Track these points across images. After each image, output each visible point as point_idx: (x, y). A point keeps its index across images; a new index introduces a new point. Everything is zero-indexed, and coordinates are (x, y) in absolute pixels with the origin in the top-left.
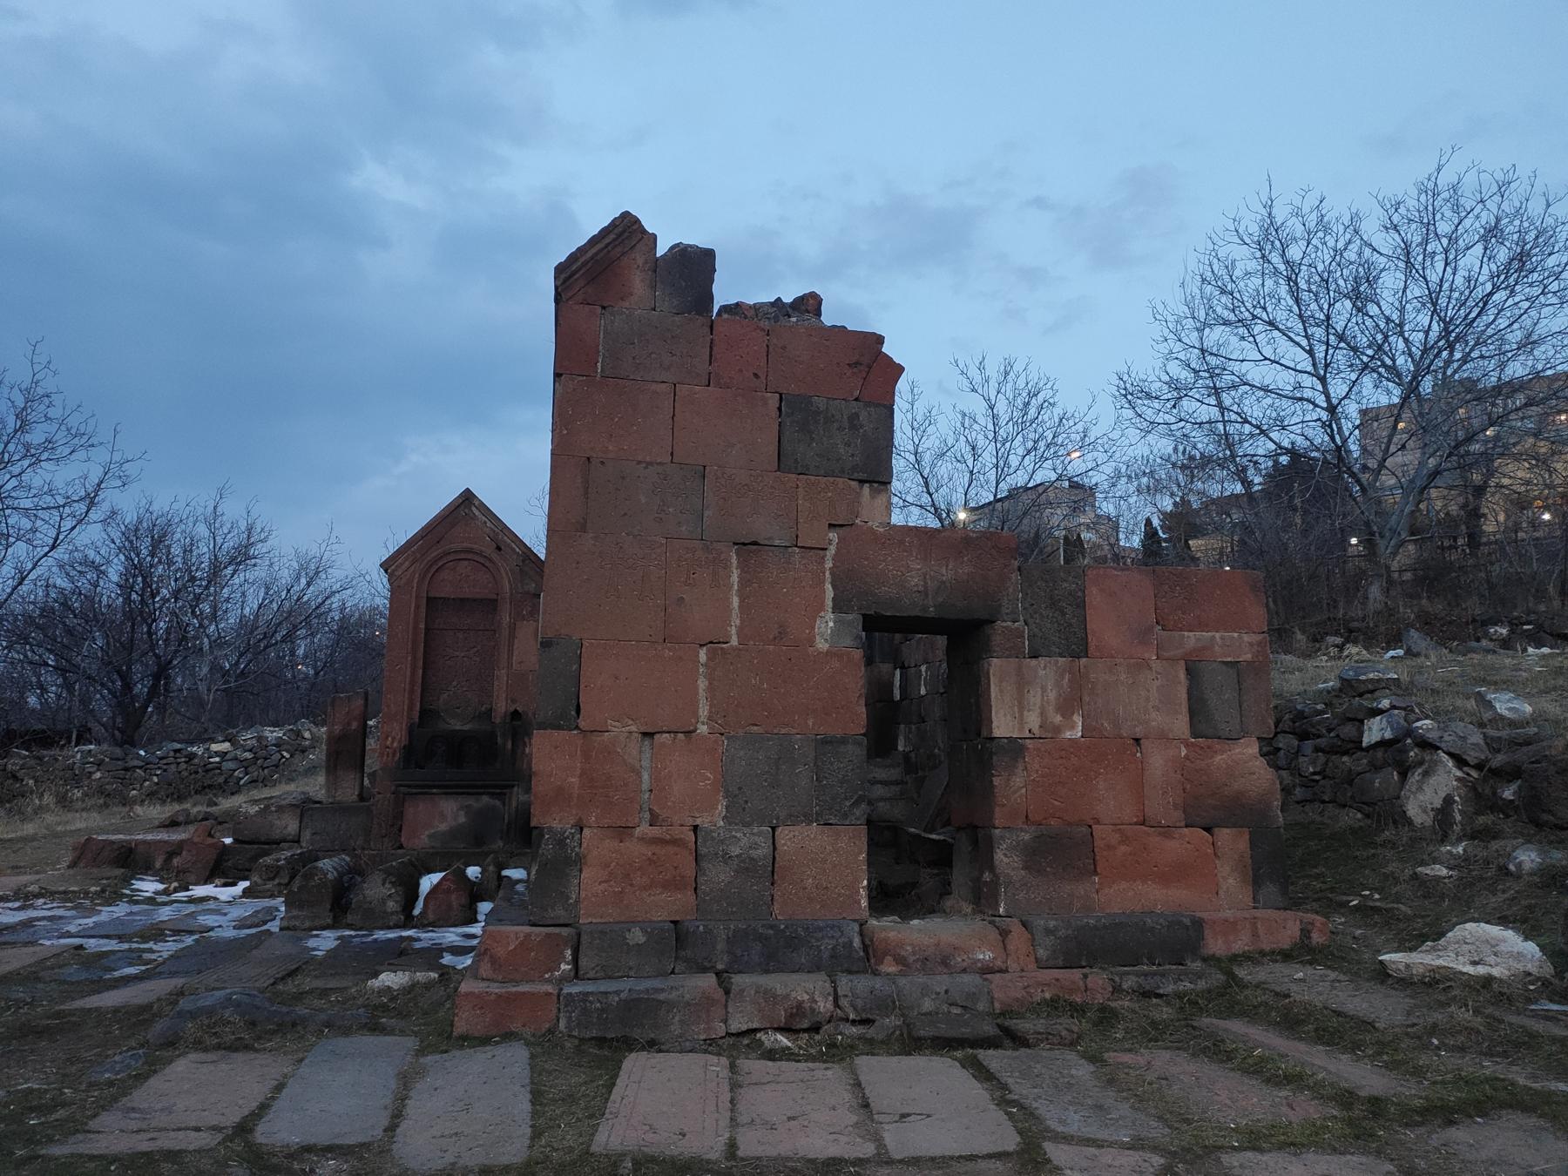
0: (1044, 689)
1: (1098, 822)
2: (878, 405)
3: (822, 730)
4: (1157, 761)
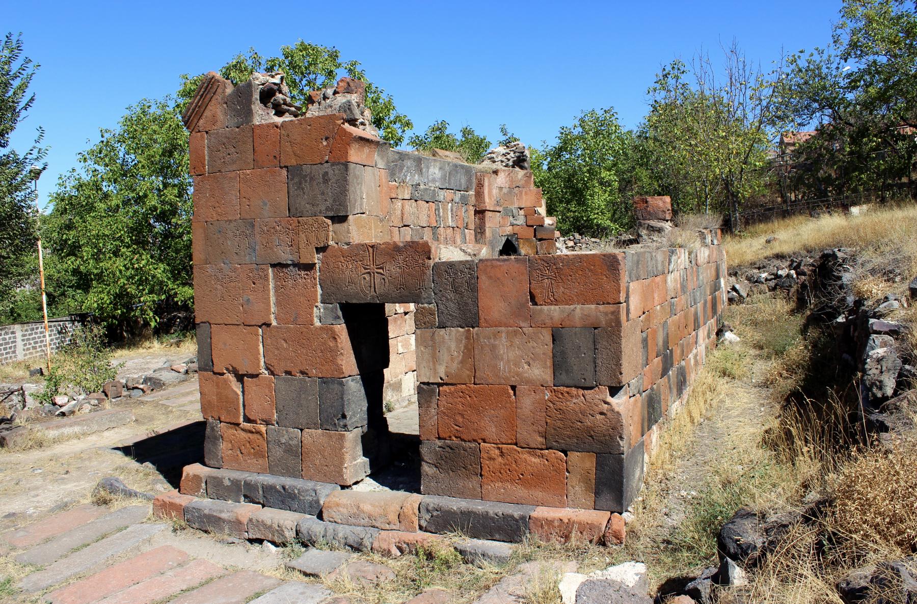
0: (449, 349)
1: (484, 442)
2: (339, 163)
3: (320, 375)
4: (527, 402)
